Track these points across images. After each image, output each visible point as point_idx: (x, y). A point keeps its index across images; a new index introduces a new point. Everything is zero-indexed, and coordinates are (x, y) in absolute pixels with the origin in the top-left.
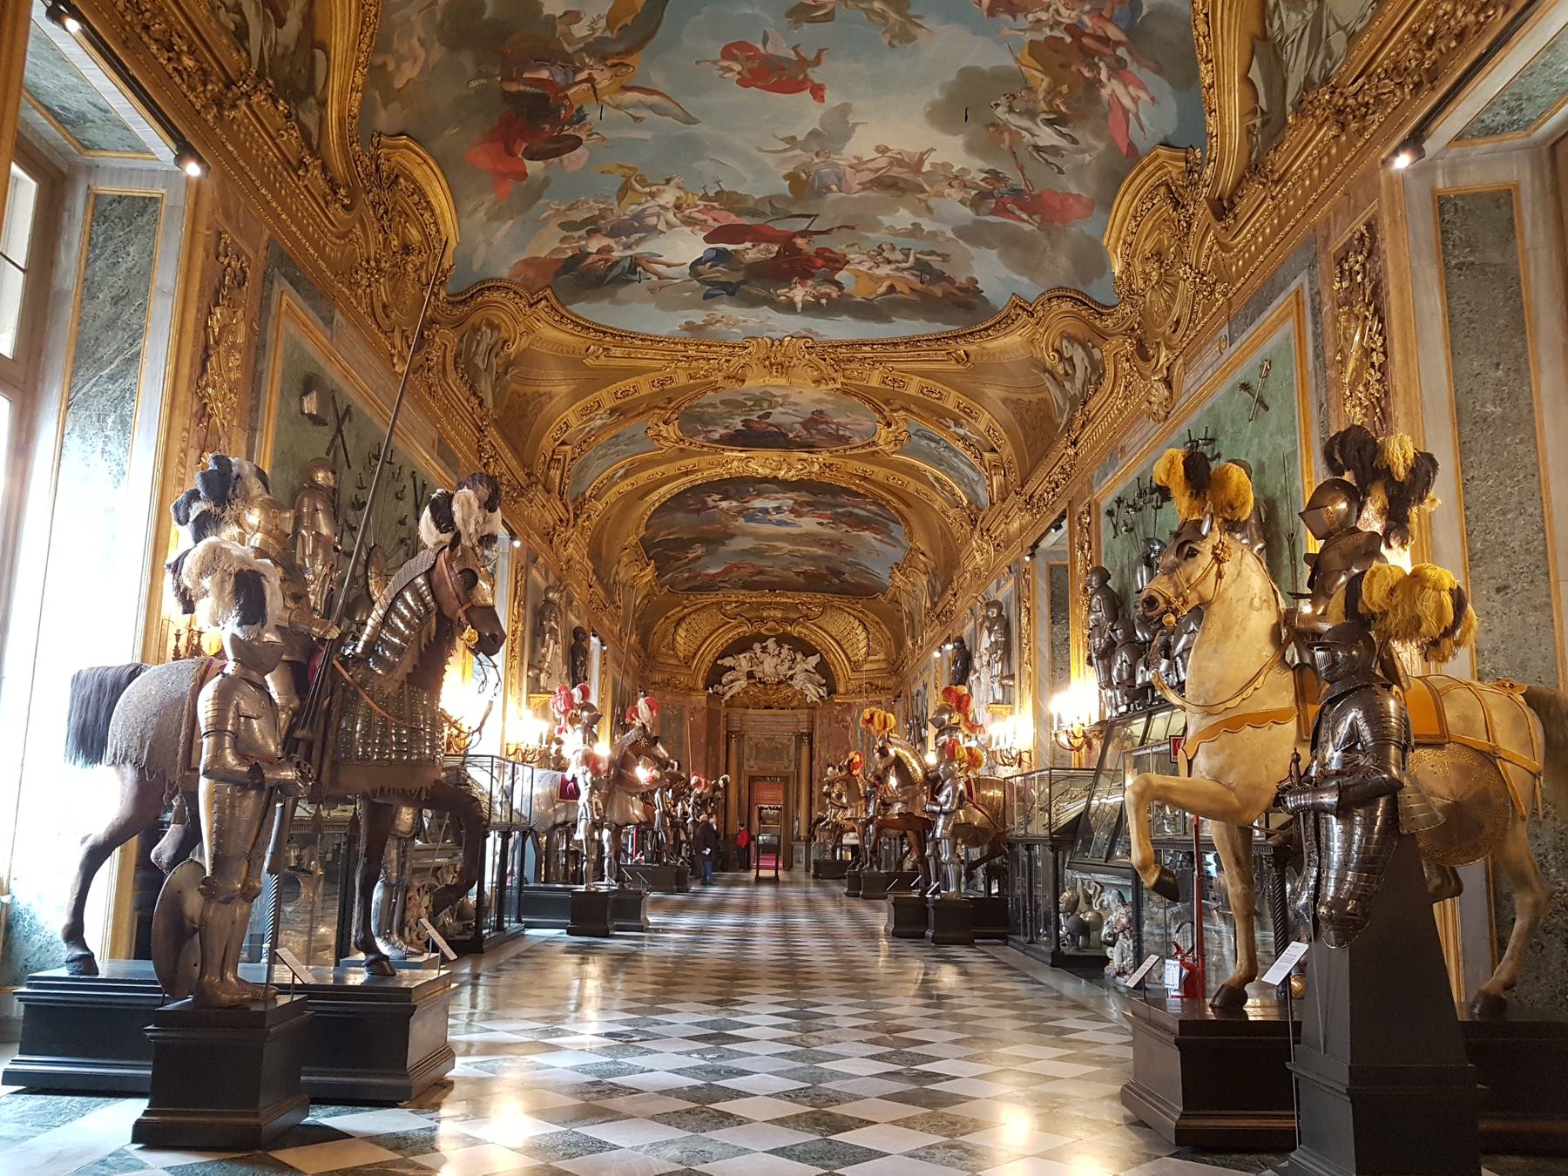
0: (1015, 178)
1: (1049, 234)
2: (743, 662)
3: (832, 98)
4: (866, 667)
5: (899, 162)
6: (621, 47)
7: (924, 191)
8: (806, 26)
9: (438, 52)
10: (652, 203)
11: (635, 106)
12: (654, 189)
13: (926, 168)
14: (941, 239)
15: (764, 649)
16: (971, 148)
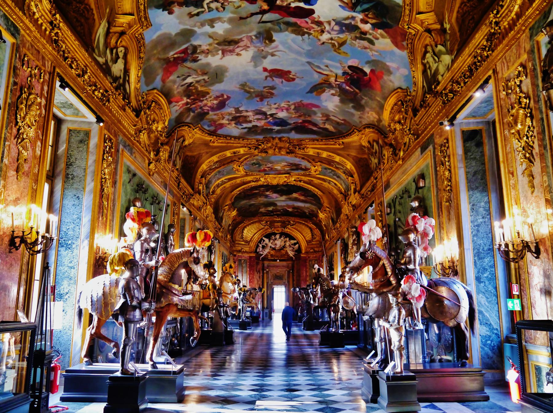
0: (189, 64)
1: (164, 60)
3: (260, 69)
5: (232, 51)
6: (324, 85)
7: (217, 44)
8: (271, 85)
9: (367, 109)
10: (333, 36)
11: (326, 70)
12: (330, 41)
13: (220, 52)
14: (199, 24)
16: (208, 64)
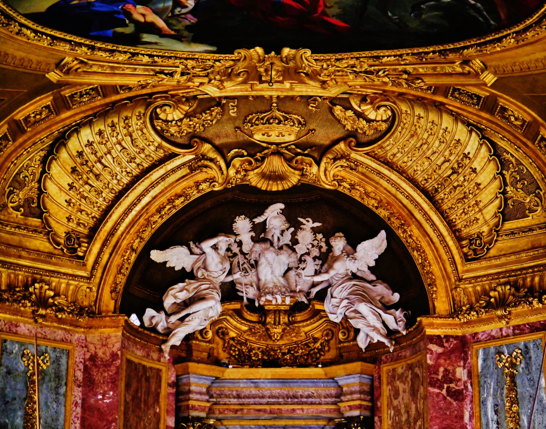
2: (212, 257)
4: (504, 244)
15: (260, 233)
